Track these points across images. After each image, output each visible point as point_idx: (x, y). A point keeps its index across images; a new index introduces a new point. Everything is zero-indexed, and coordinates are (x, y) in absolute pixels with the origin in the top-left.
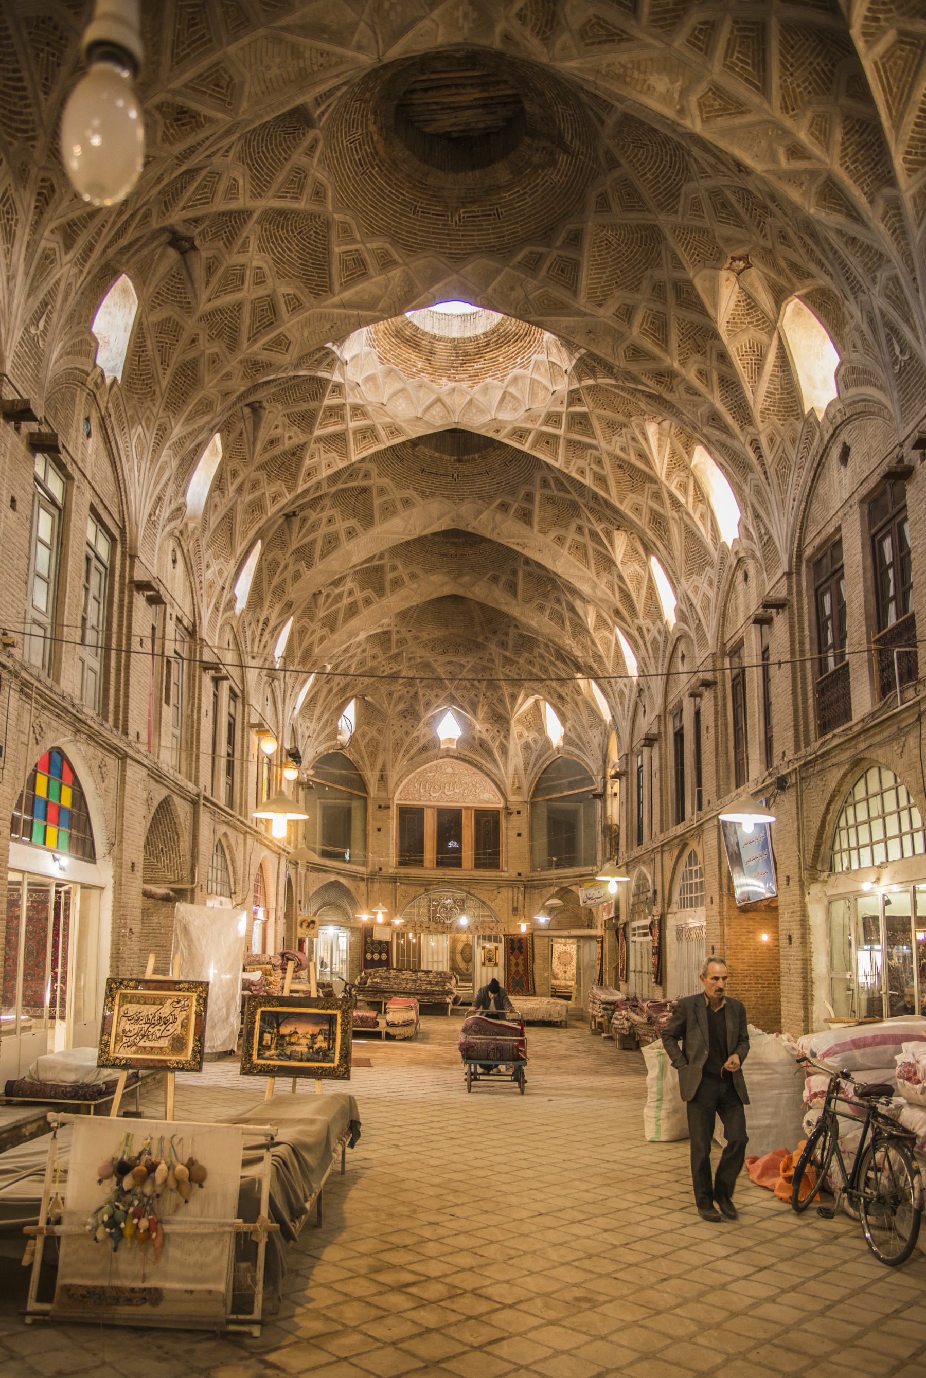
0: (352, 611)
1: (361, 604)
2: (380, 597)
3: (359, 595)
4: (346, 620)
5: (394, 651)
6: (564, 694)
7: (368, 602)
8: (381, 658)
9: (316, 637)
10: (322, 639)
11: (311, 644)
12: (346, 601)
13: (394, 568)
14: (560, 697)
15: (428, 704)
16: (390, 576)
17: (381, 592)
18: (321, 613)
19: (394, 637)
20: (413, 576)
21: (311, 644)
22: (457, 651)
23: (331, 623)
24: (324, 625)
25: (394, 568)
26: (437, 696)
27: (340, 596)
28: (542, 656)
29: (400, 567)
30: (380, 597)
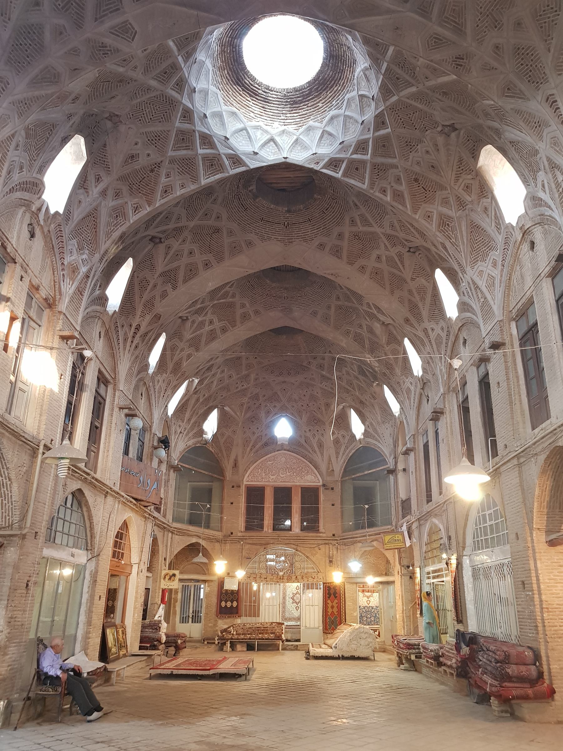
0: (212, 336)
1: (218, 332)
2: (233, 327)
3: (217, 324)
4: (207, 343)
5: (244, 372)
6: (364, 400)
7: (224, 330)
8: (235, 377)
9: (185, 353)
10: (189, 356)
11: (181, 359)
12: (207, 328)
13: (243, 306)
14: (361, 402)
15: (268, 413)
16: (239, 312)
17: (233, 324)
18: (188, 335)
19: (244, 362)
20: (257, 312)
21: (181, 359)
22: (289, 374)
23: (195, 344)
24: (190, 346)
25: (243, 306)
26: (275, 406)
27: (202, 323)
28: (348, 373)
29: (247, 305)
30: (233, 327)
